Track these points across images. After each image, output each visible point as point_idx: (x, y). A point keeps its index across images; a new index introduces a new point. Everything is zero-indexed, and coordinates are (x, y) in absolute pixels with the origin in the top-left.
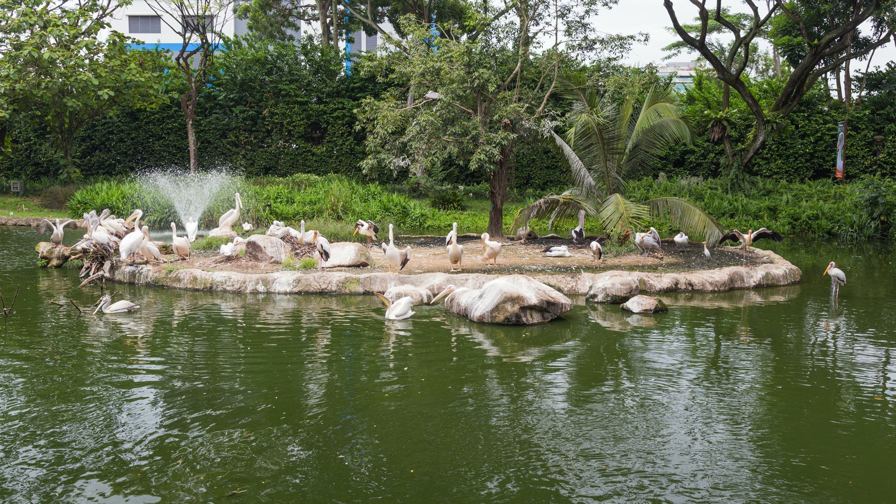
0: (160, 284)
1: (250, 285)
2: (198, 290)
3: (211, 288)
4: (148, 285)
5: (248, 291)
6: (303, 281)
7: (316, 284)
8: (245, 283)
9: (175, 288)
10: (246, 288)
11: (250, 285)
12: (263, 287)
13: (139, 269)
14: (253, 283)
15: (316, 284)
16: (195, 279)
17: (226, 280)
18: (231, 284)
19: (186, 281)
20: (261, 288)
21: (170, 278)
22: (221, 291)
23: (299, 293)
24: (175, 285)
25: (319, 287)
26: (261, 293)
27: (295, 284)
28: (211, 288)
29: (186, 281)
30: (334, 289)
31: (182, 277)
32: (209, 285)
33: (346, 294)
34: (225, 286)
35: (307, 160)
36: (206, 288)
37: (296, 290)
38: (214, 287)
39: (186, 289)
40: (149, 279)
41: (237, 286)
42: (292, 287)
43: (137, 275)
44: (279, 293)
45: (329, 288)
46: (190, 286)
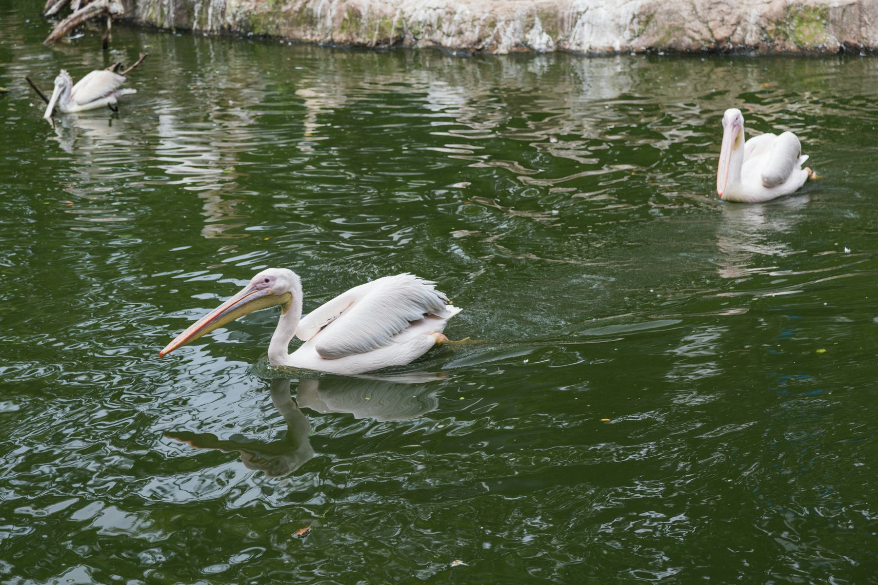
1: (510, 30)
2: (362, 48)
3: (399, 40)
4: (227, 35)
5: (502, 49)
6: (660, 18)
7: (697, 25)
8: (493, 25)
9: (299, 43)
10: (497, 39)
11: (510, 30)
12: (546, 37)
14: (518, 24)
15: (697, 25)
17: (439, 19)
18: (453, 29)
19: (329, 23)
20: (540, 40)
21: (287, 14)
23: (651, 53)
25: (707, 35)
26: (538, 54)
27: (636, 27)
28: (399, 40)
29: (329, 23)
30: (751, 39)
31: (318, 10)
32: (392, 34)
33: (787, 55)
34: (437, 36)
36: (387, 41)
37: (641, 43)
38: (408, 38)
39: (331, 47)
41: (471, 35)
42: (627, 34)
44: (591, 55)
45: (736, 38)
46: (340, 37)
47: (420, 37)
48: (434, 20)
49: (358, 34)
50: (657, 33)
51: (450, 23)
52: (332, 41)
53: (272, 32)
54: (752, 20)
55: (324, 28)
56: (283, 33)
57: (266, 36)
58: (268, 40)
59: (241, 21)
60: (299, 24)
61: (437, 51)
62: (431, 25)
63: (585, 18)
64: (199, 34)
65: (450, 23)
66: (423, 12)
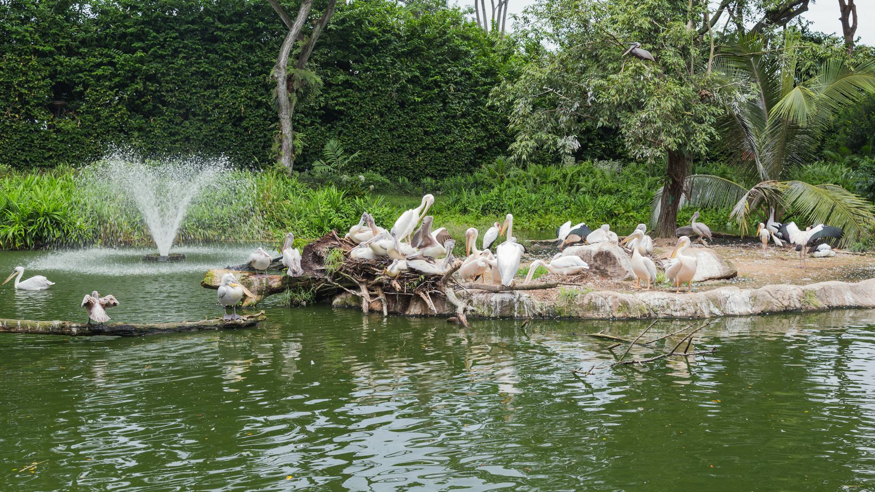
0: (565, 314)
2: (634, 319)
3: (650, 314)
9: (591, 319)
13: (517, 296)
16: (625, 304)
17: (668, 304)
18: (678, 308)
20: (717, 311)
21: (581, 306)
22: (665, 318)
23: (762, 314)
24: (590, 315)
27: (752, 303)
29: (608, 309)
31: (599, 302)
34: (668, 312)
35: (47, 139)
36: (645, 315)
38: (653, 315)
40: (539, 310)
41: (690, 311)
43: (516, 306)
45: (792, 305)
46: (618, 315)
47: (658, 312)
48: (665, 304)
50: (762, 305)
52: (614, 317)
53: (574, 314)
54: (795, 297)
56: (580, 315)
57: (570, 317)
58: (570, 319)
59: (548, 310)
60: (589, 310)
61: (670, 319)
62: (663, 307)
63: (730, 299)
64: (521, 319)
66: (656, 301)
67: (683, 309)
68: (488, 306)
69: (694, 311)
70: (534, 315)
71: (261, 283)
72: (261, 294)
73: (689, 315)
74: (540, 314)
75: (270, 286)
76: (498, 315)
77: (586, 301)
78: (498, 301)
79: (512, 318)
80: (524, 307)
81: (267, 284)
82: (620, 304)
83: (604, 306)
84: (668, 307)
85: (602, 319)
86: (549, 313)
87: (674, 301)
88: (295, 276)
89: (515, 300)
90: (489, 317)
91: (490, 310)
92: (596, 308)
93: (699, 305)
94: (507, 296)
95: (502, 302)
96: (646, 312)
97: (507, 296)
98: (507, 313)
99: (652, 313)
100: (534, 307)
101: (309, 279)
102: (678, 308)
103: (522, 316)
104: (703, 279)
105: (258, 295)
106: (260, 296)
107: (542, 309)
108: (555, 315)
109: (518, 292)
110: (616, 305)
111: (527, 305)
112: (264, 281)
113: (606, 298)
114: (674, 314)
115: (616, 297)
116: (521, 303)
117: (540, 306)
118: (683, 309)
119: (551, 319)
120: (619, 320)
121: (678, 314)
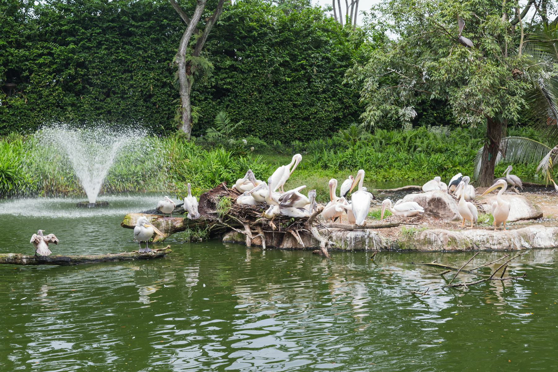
0: (405, 247)
2: (460, 251)
3: (473, 247)
10: (514, 244)
13: (368, 233)
16: (453, 240)
17: (487, 239)
18: (496, 242)
20: (527, 245)
21: (418, 241)
22: (485, 251)
27: (555, 238)
29: (440, 243)
31: (433, 238)
34: (488, 245)
36: (469, 248)
38: (476, 248)
39: (444, 251)
40: (385, 244)
41: (506, 244)
43: (367, 241)
48: (485, 240)
49: (457, 246)
51: (493, 240)
52: (444, 250)
53: (413, 248)
55: (437, 245)
56: (418, 248)
57: (410, 250)
58: (410, 251)
59: (392, 244)
60: (424, 244)
61: (489, 251)
62: (484, 241)
63: (537, 235)
64: (370, 252)
65: (493, 240)
66: (478, 237)
67: (500, 243)
68: (344, 241)
69: (508, 245)
70: (381, 248)
71: (167, 224)
72: (168, 232)
73: (505, 248)
74: (386, 248)
75: (175, 226)
76: (353, 248)
77: (422, 237)
78: (353, 237)
79: (364, 250)
80: (373, 242)
81: (172, 224)
82: (449, 240)
83: (436, 241)
84: (488, 242)
85: (435, 252)
86: (393, 247)
87: (492, 237)
88: (194, 218)
89: (366, 236)
90: (345, 249)
91: (346, 244)
92: (430, 243)
93: (512, 240)
94: (359, 234)
95: (356, 238)
96: (470, 246)
97: (359, 234)
98: (360, 246)
99: (475, 246)
100: (381, 242)
101: (204, 221)
102: (496, 242)
103: (371, 249)
104: (516, 220)
105: (165, 233)
106: (166, 234)
107: (387, 244)
108: (398, 248)
109: (368, 230)
110: (446, 240)
111: (375, 241)
112: (170, 222)
113: (438, 235)
114: (493, 247)
115: (446, 234)
116: (371, 239)
117: (385, 241)
118: (500, 243)
119: (394, 251)
120: (449, 252)
121: (496, 247)
